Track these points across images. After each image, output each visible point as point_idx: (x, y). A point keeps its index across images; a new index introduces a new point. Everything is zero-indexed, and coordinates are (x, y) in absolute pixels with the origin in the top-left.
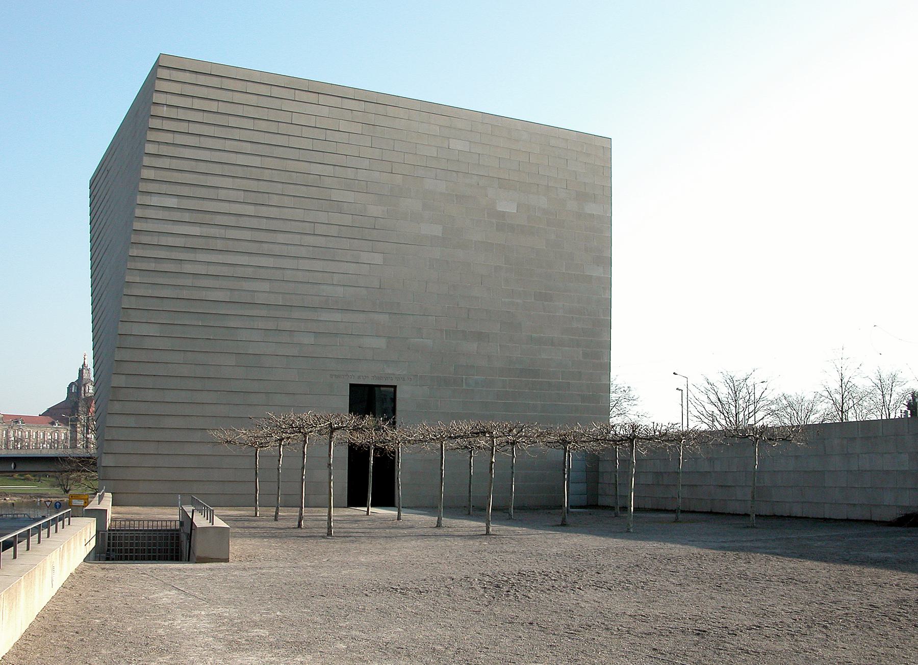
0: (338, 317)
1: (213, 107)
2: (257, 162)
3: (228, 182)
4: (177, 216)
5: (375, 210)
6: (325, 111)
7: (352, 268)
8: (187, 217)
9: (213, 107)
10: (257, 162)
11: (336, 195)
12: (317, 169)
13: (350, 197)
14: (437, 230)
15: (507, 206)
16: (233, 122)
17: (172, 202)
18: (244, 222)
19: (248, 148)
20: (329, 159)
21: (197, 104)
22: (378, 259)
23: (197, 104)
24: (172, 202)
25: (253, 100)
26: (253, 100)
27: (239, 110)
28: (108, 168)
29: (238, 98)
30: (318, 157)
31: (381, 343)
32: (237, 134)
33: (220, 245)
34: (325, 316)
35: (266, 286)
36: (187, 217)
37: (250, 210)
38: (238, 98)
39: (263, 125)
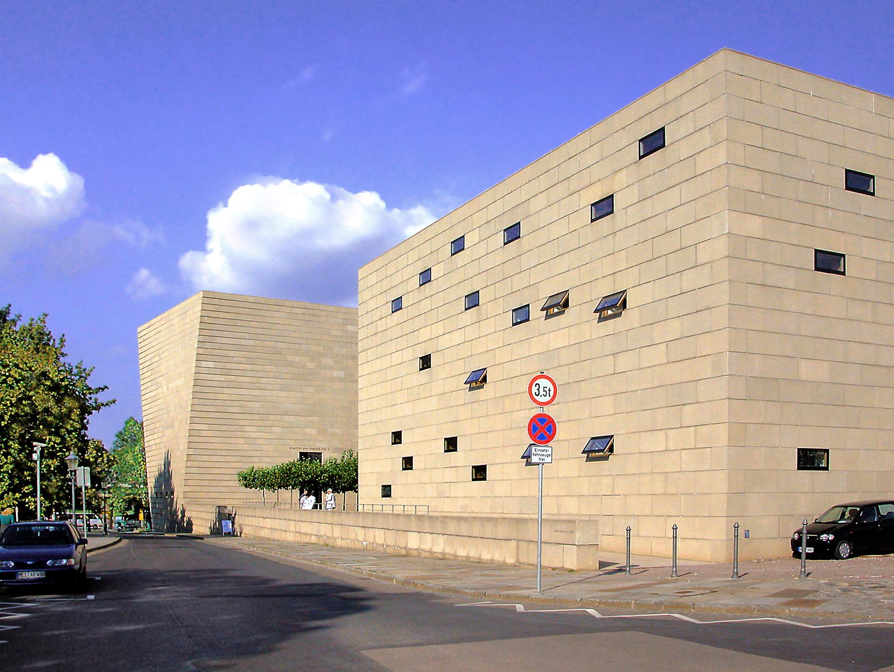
0: (292, 418)
1: (229, 316)
2: (252, 343)
3: (237, 354)
5: (310, 365)
7: (298, 394)
9: (229, 316)
10: (252, 343)
11: (290, 358)
13: (297, 359)
14: (341, 374)
16: (239, 323)
17: (211, 364)
18: (246, 373)
19: (247, 336)
20: (286, 340)
21: (221, 315)
22: (311, 390)
23: (221, 315)
24: (211, 364)
27: (243, 317)
28: (159, 329)
30: (281, 339)
31: (314, 431)
32: (241, 329)
33: (233, 385)
34: (286, 418)
35: (258, 405)
37: (249, 367)
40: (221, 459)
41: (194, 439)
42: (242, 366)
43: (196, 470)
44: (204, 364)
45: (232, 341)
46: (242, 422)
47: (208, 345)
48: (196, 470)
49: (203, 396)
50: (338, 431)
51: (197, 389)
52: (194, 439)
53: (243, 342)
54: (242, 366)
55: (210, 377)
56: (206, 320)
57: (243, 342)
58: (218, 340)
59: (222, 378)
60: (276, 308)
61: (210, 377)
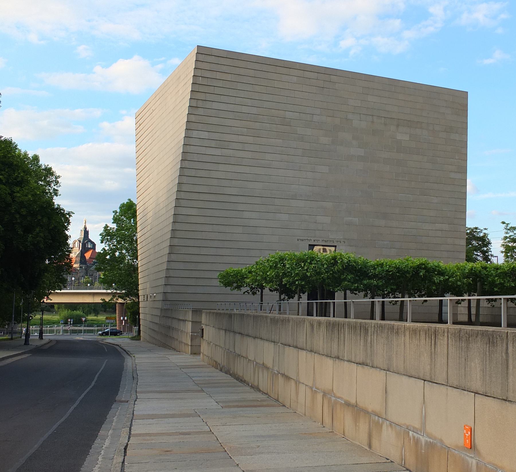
1: (229, 77)
2: (254, 110)
4: (206, 143)
6: (295, 79)
8: (213, 144)
9: (229, 77)
10: (254, 110)
12: (289, 115)
15: (403, 136)
16: (240, 86)
17: (205, 135)
21: (219, 76)
23: (219, 76)
24: (205, 135)
25: (252, 73)
26: (252, 73)
29: (242, 71)
36: (213, 144)
37: (250, 140)
38: (242, 71)
39: (257, 88)
40: (213, 251)
41: (178, 226)
42: (241, 138)
43: (182, 266)
44: (195, 134)
45: (231, 107)
46: (240, 207)
47: (201, 111)
48: (182, 266)
49: (193, 173)
50: (356, 220)
51: (186, 164)
52: (178, 226)
53: (244, 109)
54: (241, 138)
55: (203, 150)
56: (200, 80)
57: (244, 109)
58: (215, 105)
59: (218, 152)
60: (285, 71)
61: (203, 150)
